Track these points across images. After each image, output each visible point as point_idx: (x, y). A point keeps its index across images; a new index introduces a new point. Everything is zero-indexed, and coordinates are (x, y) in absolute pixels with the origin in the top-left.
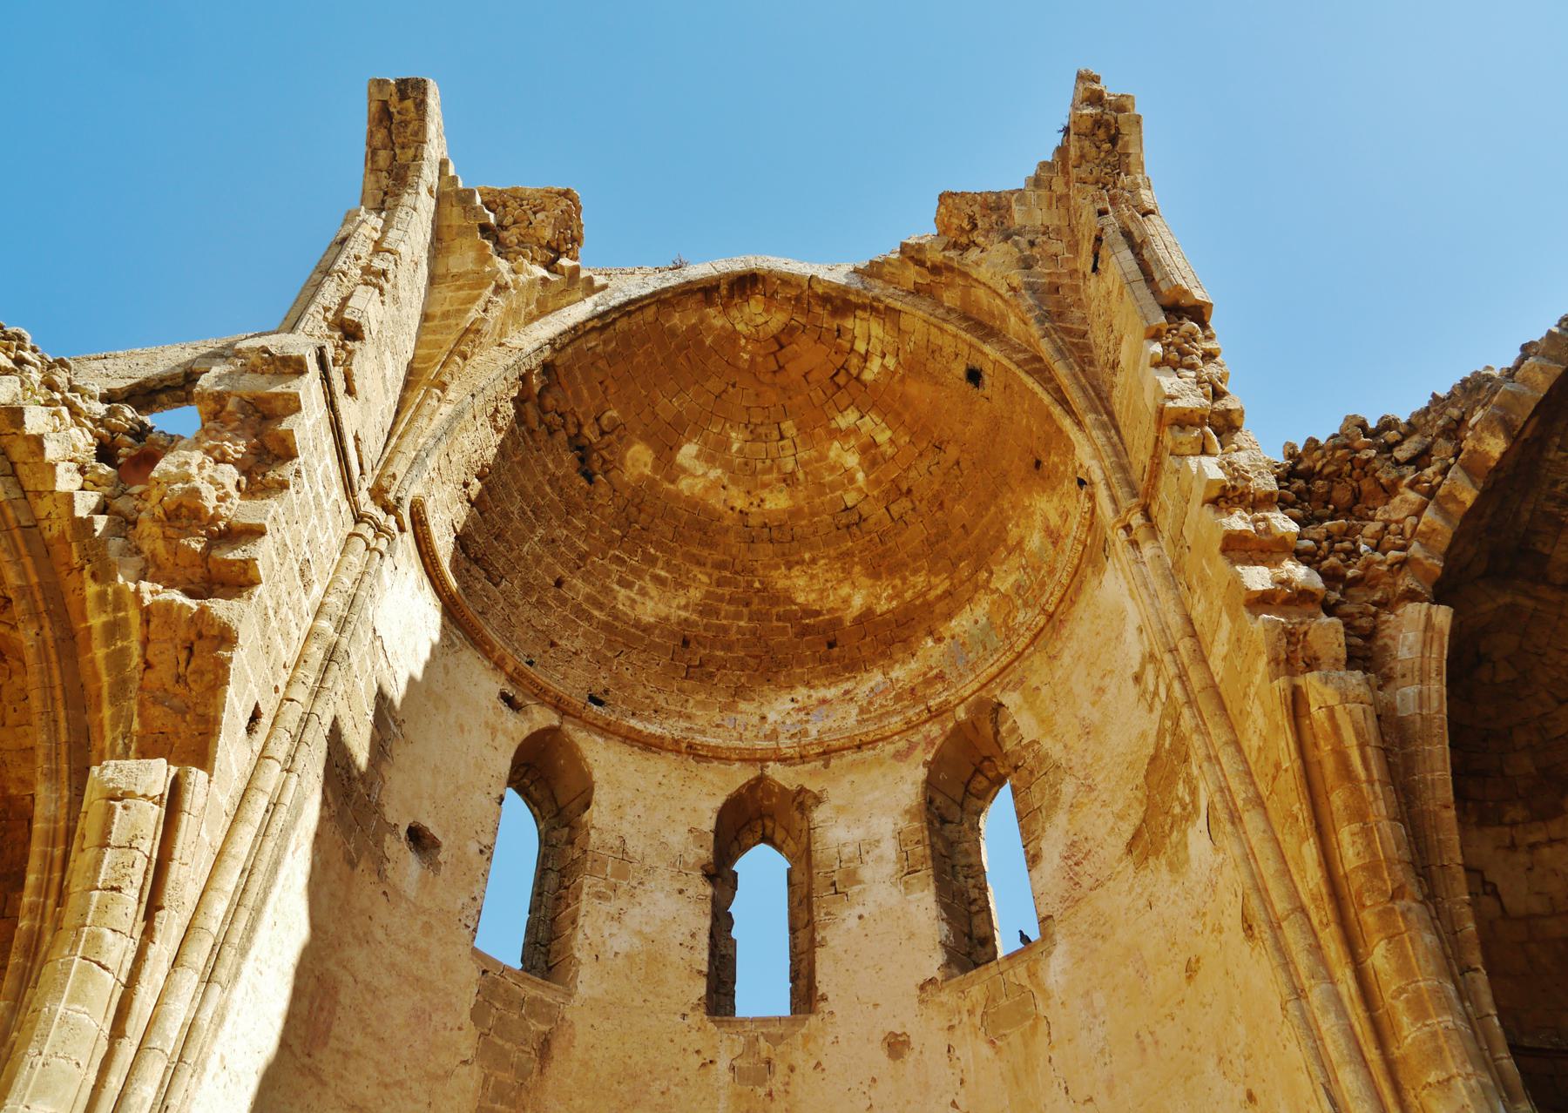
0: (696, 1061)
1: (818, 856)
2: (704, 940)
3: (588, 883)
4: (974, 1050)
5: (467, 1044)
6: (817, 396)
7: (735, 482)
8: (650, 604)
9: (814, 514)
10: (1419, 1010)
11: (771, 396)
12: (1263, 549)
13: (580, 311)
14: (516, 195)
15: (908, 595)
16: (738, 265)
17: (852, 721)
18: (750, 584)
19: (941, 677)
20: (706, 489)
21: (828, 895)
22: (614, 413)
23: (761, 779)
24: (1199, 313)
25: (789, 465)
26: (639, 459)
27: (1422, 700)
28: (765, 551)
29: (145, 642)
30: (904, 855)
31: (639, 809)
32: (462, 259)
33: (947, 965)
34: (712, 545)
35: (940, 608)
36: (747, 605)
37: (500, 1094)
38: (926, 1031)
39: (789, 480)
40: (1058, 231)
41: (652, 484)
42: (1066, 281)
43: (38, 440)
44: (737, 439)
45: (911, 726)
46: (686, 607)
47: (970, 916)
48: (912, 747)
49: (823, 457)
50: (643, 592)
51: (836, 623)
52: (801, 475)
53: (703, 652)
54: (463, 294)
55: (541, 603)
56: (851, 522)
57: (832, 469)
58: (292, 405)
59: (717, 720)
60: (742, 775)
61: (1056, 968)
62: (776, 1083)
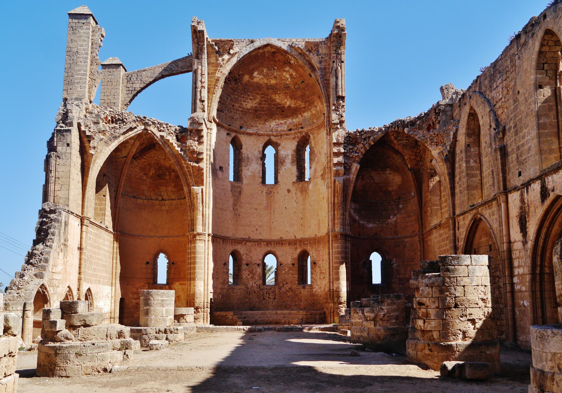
0: (261, 191)
1: (279, 156)
2: (261, 172)
3: (244, 164)
4: (299, 194)
5: (230, 195)
6: (281, 63)
7: (265, 78)
8: (249, 104)
9: (280, 84)
10: (337, 219)
11: (272, 63)
12: (337, 154)
13: (234, 60)
14: (221, 41)
15: (297, 105)
16: (265, 43)
17: (286, 129)
18: (268, 98)
19: (301, 124)
20: (259, 80)
21: (280, 164)
22: (241, 72)
23: (270, 139)
24: (343, 98)
25: (276, 75)
26: (246, 78)
27: (353, 177)
28: (271, 91)
29: (192, 170)
30: (292, 159)
31: (250, 148)
32: (213, 60)
33: (297, 180)
34: (260, 90)
35: (303, 109)
36: (267, 102)
37: (235, 200)
38: (293, 189)
39: (275, 78)
40: (328, 54)
41: (249, 81)
42: (327, 67)
43: (172, 144)
44: (265, 70)
45: (295, 133)
46: (256, 104)
47: (302, 170)
48: (295, 137)
49: (282, 74)
50: (248, 102)
51: (284, 107)
52: (278, 77)
53: (259, 112)
54: (214, 68)
55: (231, 111)
56: (287, 87)
57: (284, 77)
58: (202, 130)
59: (262, 127)
60: (267, 139)
61: (311, 186)
62: (272, 195)
